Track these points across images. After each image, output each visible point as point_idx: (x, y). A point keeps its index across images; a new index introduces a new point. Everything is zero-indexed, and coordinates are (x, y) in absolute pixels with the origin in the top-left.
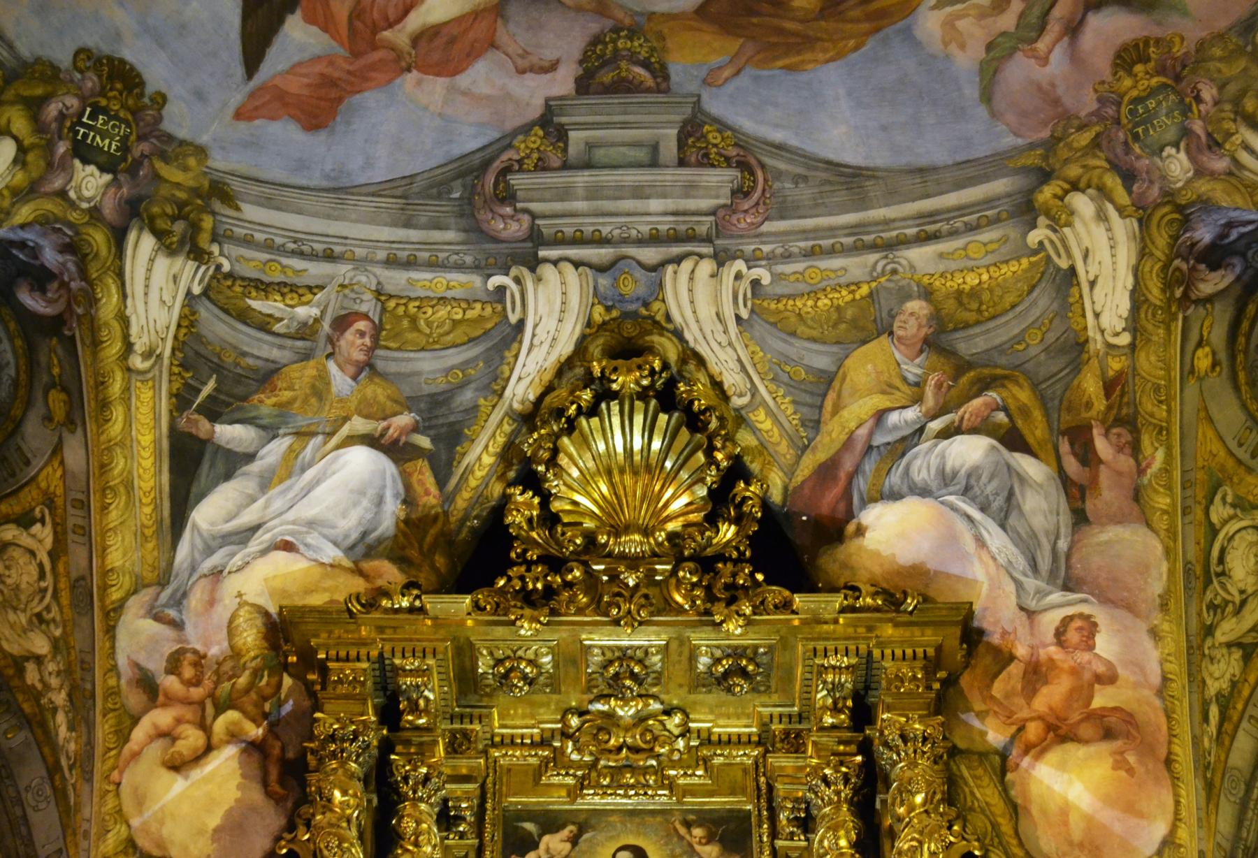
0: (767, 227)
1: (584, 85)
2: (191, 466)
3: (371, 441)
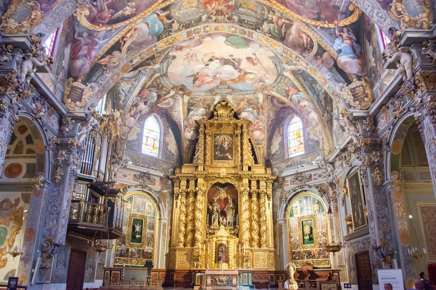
1: (220, 84)
2: (189, 110)
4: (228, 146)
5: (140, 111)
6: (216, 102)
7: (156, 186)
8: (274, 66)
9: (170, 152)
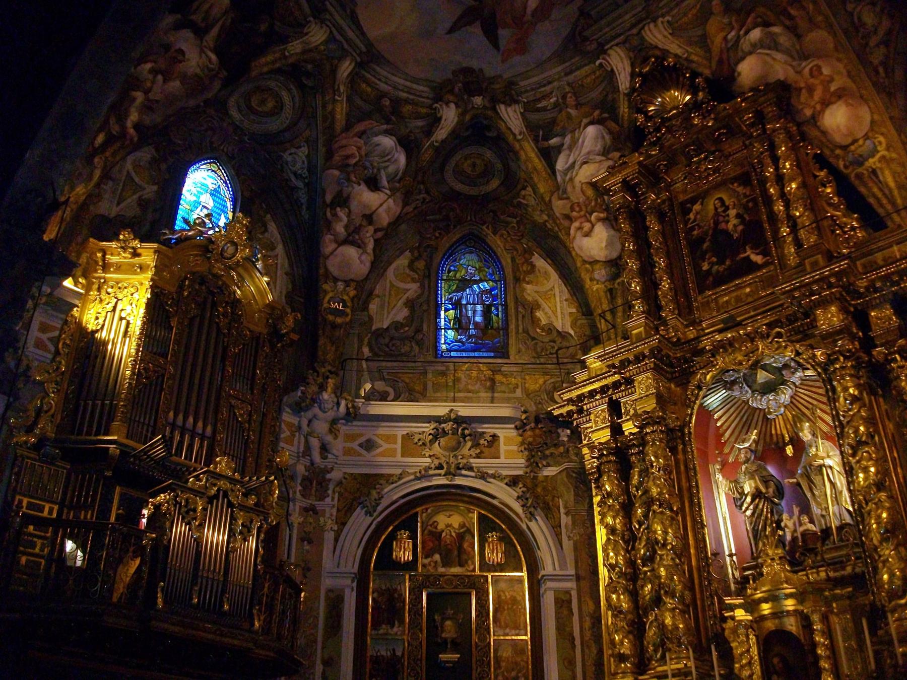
0: (660, 5)
2: (549, 156)
4: (743, 222)
5: (369, 218)
6: (624, 81)
7: (502, 460)
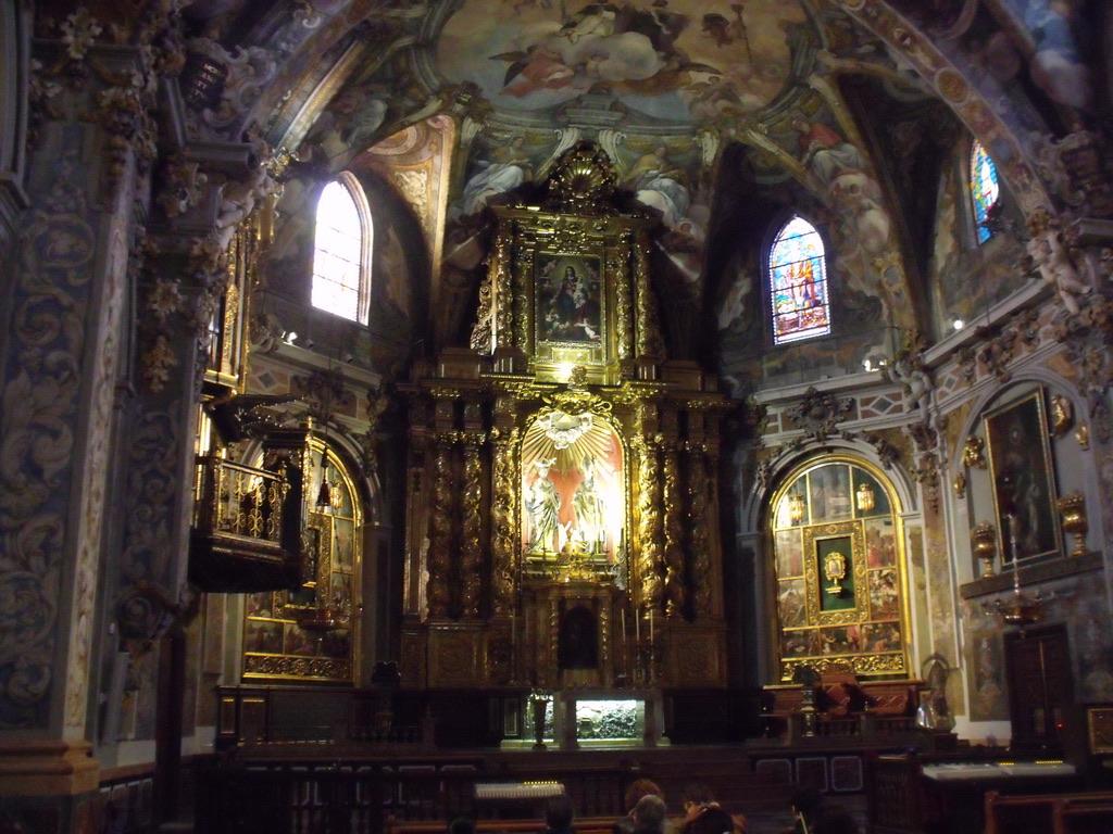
1: (589, 92)
3: (518, 165)
4: (586, 297)
8: (786, 51)
9: (394, 305)
